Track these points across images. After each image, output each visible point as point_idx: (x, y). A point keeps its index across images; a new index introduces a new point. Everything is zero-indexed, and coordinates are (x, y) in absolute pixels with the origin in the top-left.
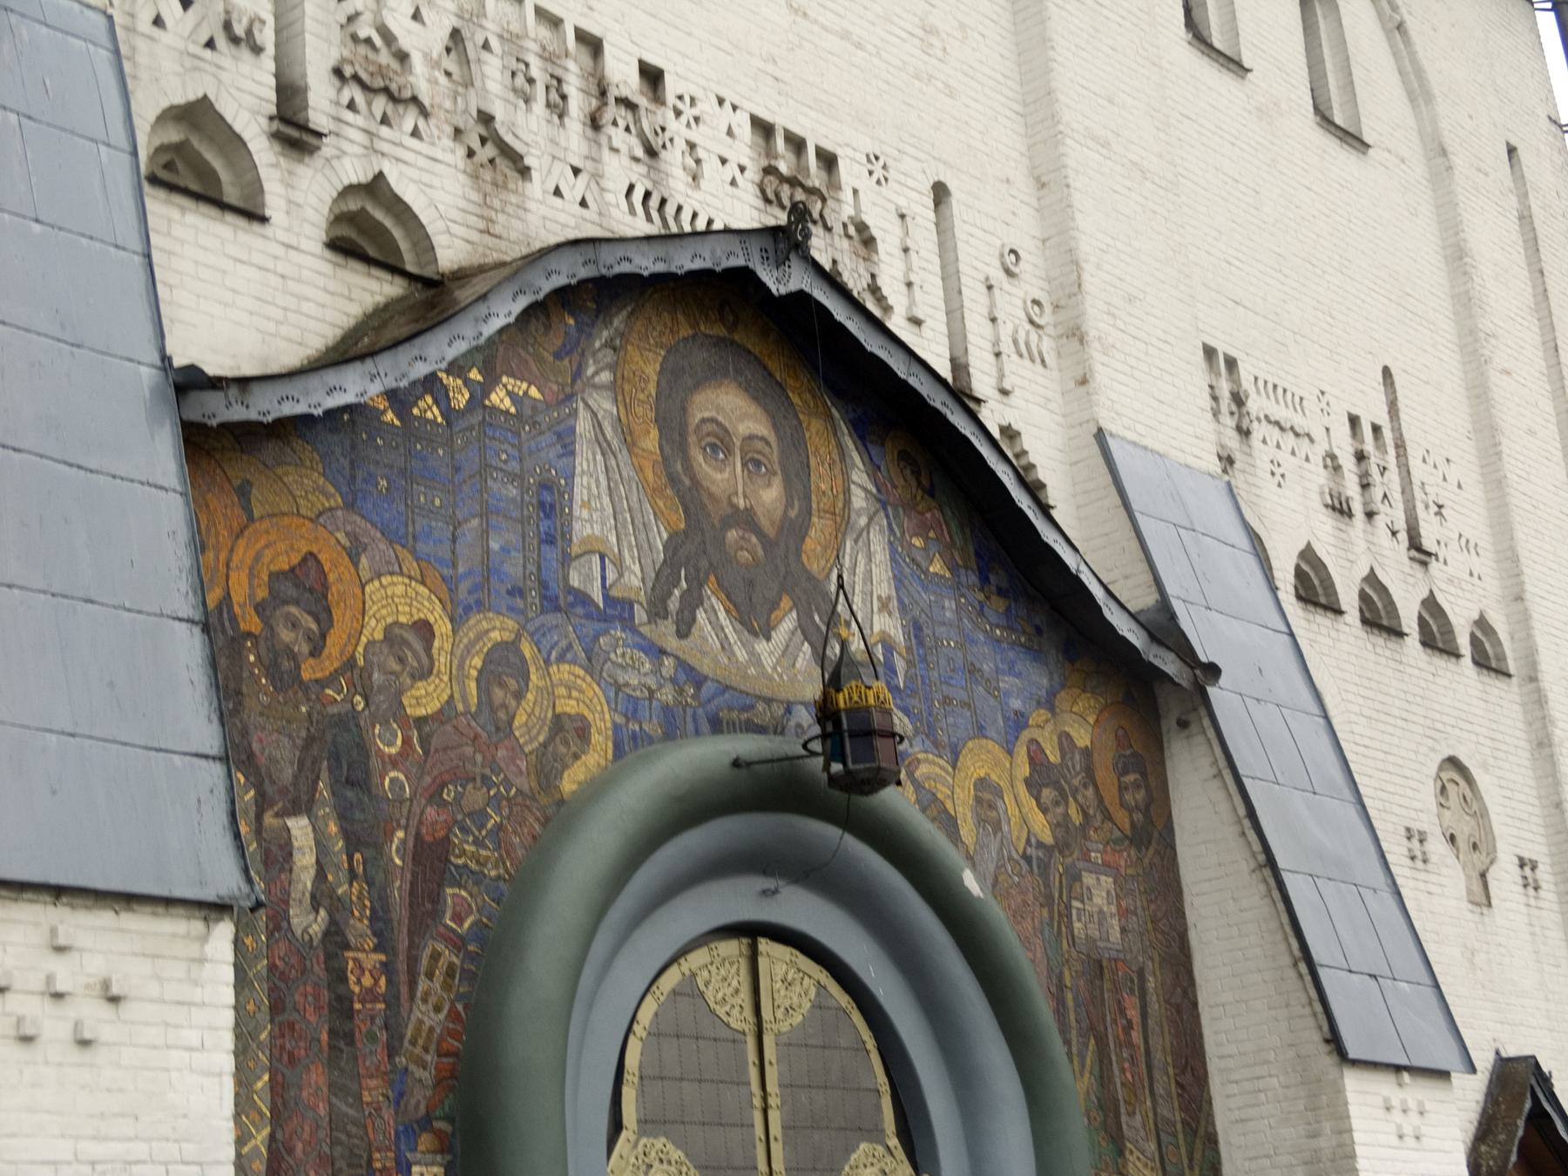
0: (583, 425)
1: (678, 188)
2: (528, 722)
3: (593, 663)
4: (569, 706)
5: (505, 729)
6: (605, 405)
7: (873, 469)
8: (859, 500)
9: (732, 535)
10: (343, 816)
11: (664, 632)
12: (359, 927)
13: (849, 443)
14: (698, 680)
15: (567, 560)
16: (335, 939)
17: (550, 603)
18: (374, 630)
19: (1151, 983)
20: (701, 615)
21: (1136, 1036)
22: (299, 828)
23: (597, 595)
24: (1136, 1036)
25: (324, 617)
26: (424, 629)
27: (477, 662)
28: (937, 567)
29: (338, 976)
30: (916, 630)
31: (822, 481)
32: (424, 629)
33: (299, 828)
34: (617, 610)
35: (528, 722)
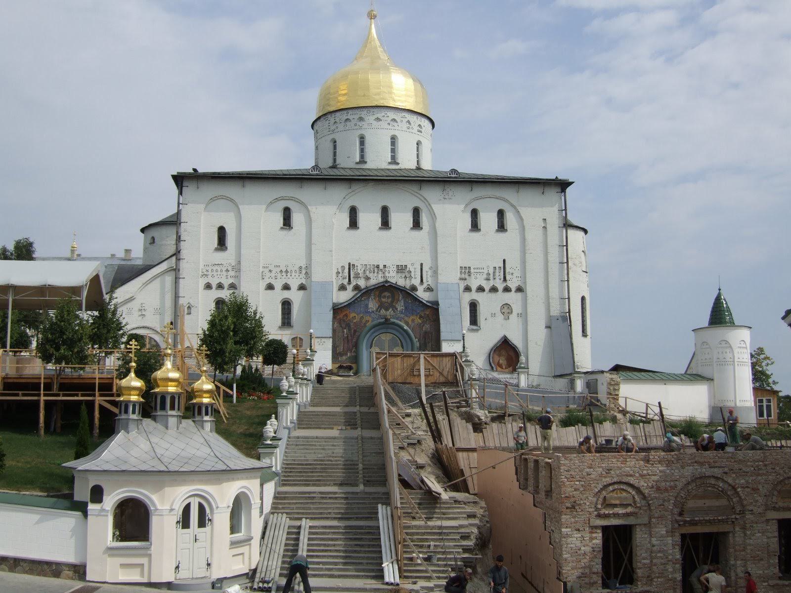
1: (387, 274)
2: (364, 321)
6: (373, 297)
12: (349, 336)
14: (380, 316)
16: (348, 336)
17: (366, 312)
21: (430, 338)
24: (430, 338)
25: (347, 318)
26: (355, 317)
29: (348, 338)
30: (406, 308)
31: (396, 297)
32: (355, 317)
34: (373, 312)
35: (364, 321)
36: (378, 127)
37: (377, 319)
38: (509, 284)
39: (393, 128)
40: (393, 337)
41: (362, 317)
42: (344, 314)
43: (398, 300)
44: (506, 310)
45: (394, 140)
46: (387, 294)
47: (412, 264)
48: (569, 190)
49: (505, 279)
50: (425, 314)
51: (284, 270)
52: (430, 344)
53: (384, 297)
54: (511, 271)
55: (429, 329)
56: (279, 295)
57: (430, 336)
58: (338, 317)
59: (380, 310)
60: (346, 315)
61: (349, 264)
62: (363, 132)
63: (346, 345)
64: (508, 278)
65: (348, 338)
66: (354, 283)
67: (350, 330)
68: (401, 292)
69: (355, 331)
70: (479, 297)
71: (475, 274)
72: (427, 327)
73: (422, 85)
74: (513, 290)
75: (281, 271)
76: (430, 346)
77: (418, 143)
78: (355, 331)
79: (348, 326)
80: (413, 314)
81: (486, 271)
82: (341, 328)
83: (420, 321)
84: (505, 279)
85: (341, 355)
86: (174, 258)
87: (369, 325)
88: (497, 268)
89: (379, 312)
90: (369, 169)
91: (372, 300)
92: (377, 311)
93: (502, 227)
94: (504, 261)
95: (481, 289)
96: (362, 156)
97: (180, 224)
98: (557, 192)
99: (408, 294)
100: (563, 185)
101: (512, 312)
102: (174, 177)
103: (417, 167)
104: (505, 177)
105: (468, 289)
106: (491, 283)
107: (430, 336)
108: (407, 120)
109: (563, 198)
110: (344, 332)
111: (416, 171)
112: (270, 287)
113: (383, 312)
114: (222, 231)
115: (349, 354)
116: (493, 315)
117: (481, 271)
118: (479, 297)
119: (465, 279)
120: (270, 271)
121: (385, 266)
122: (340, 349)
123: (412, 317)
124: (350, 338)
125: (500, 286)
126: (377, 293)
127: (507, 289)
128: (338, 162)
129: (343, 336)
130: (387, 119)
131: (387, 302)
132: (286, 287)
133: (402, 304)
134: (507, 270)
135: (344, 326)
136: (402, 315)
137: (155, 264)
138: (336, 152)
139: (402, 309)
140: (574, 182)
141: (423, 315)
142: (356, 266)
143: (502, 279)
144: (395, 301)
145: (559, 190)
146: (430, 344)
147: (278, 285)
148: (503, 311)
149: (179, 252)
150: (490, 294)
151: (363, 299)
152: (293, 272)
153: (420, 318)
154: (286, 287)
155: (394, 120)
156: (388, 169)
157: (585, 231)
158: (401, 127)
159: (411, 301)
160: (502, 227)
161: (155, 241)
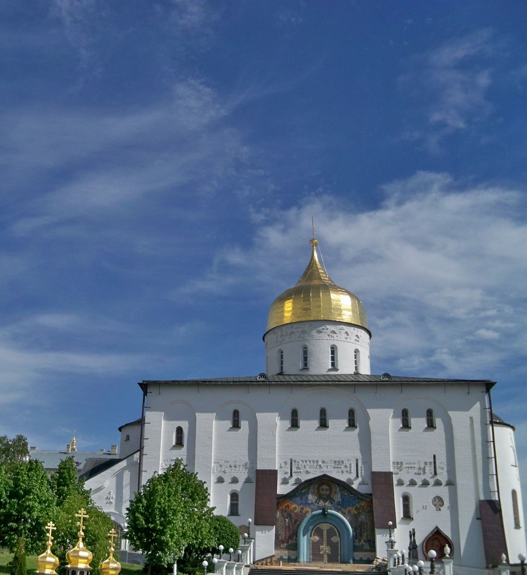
0: (310, 491)
2: (304, 511)
3: (309, 507)
4: (307, 510)
5: (302, 512)
6: (312, 490)
7: (339, 488)
8: (337, 491)
9: (324, 496)
10: (290, 518)
11: (316, 504)
12: (291, 525)
13: (337, 487)
15: (308, 501)
16: (289, 525)
17: (306, 504)
18: (292, 508)
19: (368, 523)
20: (320, 502)
22: (287, 520)
23: (310, 503)
24: (366, 528)
25: (289, 508)
26: (296, 507)
27: (300, 509)
28: (346, 494)
29: (289, 527)
30: (343, 500)
31: (333, 490)
32: (296, 507)
33: (287, 520)
34: (312, 503)
36: (320, 338)
37: (316, 510)
38: (438, 477)
39: (332, 338)
40: (331, 528)
41: (302, 509)
42: (286, 504)
43: (336, 492)
44: (438, 501)
45: (333, 350)
46: (325, 487)
47: (348, 460)
48: (492, 391)
49: (435, 473)
50: (360, 506)
51: (233, 465)
52: (365, 533)
53: (323, 490)
54: (441, 465)
55: (364, 520)
56: (228, 488)
57: (366, 526)
58: (281, 508)
59: (319, 501)
60: (288, 506)
61: (291, 460)
62: (336, 343)
63: (288, 533)
64: (438, 471)
65: (289, 527)
66: (295, 477)
67: (291, 520)
68: (338, 485)
69: (296, 521)
70: (411, 491)
71: (407, 469)
72: (362, 518)
73: (357, 299)
74: (444, 483)
75: (231, 466)
76: (366, 535)
77: (357, 351)
78: (296, 521)
79: (289, 516)
80: (349, 506)
81: (417, 466)
82: (283, 518)
83: (356, 512)
84: (435, 473)
85: (283, 542)
86: (138, 453)
87: (309, 516)
88: (428, 463)
89: (318, 503)
90: (312, 376)
91: (311, 492)
92: (316, 502)
93: (431, 425)
94: (434, 456)
95: (413, 483)
96: (306, 364)
97: (144, 424)
98: (482, 392)
99: (345, 486)
100: (488, 385)
101: (443, 505)
102: (140, 384)
103: (354, 372)
104: (433, 380)
105: (400, 483)
106: (423, 477)
107: (366, 526)
108: (344, 331)
109: (486, 398)
110: (286, 521)
111: (354, 376)
112: (220, 480)
113: (321, 503)
114: (179, 431)
115: (290, 542)
116: (425, 508)
117: (412, 466)
118: (411, 491)
119: (398, 474)
120: (221, 466)
121: (323, 462)
122: (282, 537)
123: (348, 508)
124: (291, 526)
125: (432, 481)
126: (316, 486)
127: (438, 483)
128: (284, 370)
129: (285, 525)
130: (326, 331)
131: (326, 495)
132: (235, 481)
133: (339, 496)
134: (438, 465)
135: (285, 515)
136: (339, 507)
137: (123, 458)
138: (283, 360)
139: (339, 501)
140: (496, 383)
141: (358, 506)
142: (297, 461)
143: (433, 473)
144: (333, 494)
145: (484, 390)
146: (365, 533)
147: (228, 479)
148: (435, 503)
149: (143, 448)
150: (421, 489)
151: (303, 491)
152: (241, 467)
153: (355, 510)
154: (235, 481)
155: (334, 332)
156: (328, 375)
157: (512, 427)
158: (340, 338)
159: (348, 494)
160: (431, 425)
161: (130, 439)
